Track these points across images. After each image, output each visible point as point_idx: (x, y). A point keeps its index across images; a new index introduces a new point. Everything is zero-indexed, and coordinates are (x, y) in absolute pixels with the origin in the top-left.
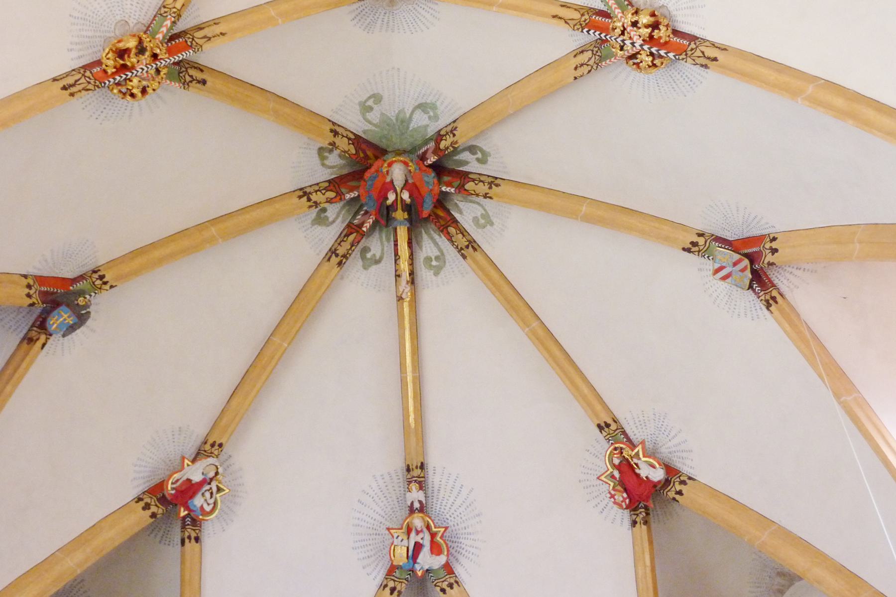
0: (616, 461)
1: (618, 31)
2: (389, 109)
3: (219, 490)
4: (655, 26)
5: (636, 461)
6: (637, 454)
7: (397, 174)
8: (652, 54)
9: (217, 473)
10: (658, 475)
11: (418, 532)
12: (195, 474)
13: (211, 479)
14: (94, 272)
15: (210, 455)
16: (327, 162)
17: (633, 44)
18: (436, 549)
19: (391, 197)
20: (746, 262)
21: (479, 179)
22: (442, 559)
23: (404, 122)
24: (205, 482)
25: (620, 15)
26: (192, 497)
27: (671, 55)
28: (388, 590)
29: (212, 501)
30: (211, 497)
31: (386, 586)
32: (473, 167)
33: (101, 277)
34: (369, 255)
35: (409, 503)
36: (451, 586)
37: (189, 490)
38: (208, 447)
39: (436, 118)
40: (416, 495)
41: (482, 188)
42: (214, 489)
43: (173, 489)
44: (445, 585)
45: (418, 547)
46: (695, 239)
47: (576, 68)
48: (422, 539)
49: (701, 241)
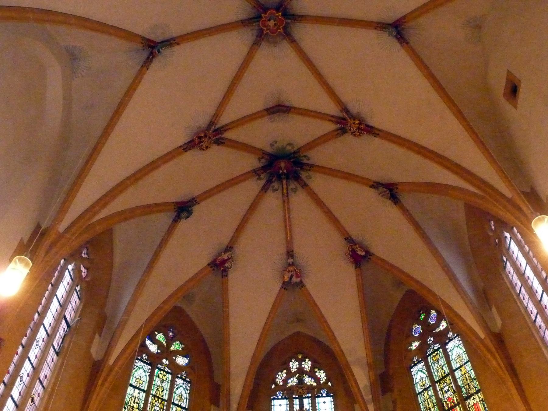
0: (351, 250)
1: (349, 125)
2: (279, 145)
4: (360, 124)
5: (356, 249)
6: (357, 247)
7: (283, 165)
8: (359, 132)
10: (363, 254)
11: (292, 272)
12: (225, 257)
13: (230, 258)
14: (193, 199)
15: (230, 251)
16: (261, 161)
17: (353, 129)
18: (297, 276)
19: (281, 172)
20: (388, 192)
21: (308, 165)
23: (284, 148)
24: (229, 259)
25: (349, 120)
26: (225, 264)
28: (283, 289)
29: (230, 265)
30: (230, 263)
32: (305, 161)
33: (195, 201)
34: (274, 188)
37: (224, 262)
38: (228, 248)
39: (293, 147)
40: (291, 260)
41: (308, 168)
42: (231, 261)
43: (219, 262)
44: (300, 287)
45: (292, 276)
46: (373, 184)
47: (336, 135)
48: (293, 273)
49: (375, 184)
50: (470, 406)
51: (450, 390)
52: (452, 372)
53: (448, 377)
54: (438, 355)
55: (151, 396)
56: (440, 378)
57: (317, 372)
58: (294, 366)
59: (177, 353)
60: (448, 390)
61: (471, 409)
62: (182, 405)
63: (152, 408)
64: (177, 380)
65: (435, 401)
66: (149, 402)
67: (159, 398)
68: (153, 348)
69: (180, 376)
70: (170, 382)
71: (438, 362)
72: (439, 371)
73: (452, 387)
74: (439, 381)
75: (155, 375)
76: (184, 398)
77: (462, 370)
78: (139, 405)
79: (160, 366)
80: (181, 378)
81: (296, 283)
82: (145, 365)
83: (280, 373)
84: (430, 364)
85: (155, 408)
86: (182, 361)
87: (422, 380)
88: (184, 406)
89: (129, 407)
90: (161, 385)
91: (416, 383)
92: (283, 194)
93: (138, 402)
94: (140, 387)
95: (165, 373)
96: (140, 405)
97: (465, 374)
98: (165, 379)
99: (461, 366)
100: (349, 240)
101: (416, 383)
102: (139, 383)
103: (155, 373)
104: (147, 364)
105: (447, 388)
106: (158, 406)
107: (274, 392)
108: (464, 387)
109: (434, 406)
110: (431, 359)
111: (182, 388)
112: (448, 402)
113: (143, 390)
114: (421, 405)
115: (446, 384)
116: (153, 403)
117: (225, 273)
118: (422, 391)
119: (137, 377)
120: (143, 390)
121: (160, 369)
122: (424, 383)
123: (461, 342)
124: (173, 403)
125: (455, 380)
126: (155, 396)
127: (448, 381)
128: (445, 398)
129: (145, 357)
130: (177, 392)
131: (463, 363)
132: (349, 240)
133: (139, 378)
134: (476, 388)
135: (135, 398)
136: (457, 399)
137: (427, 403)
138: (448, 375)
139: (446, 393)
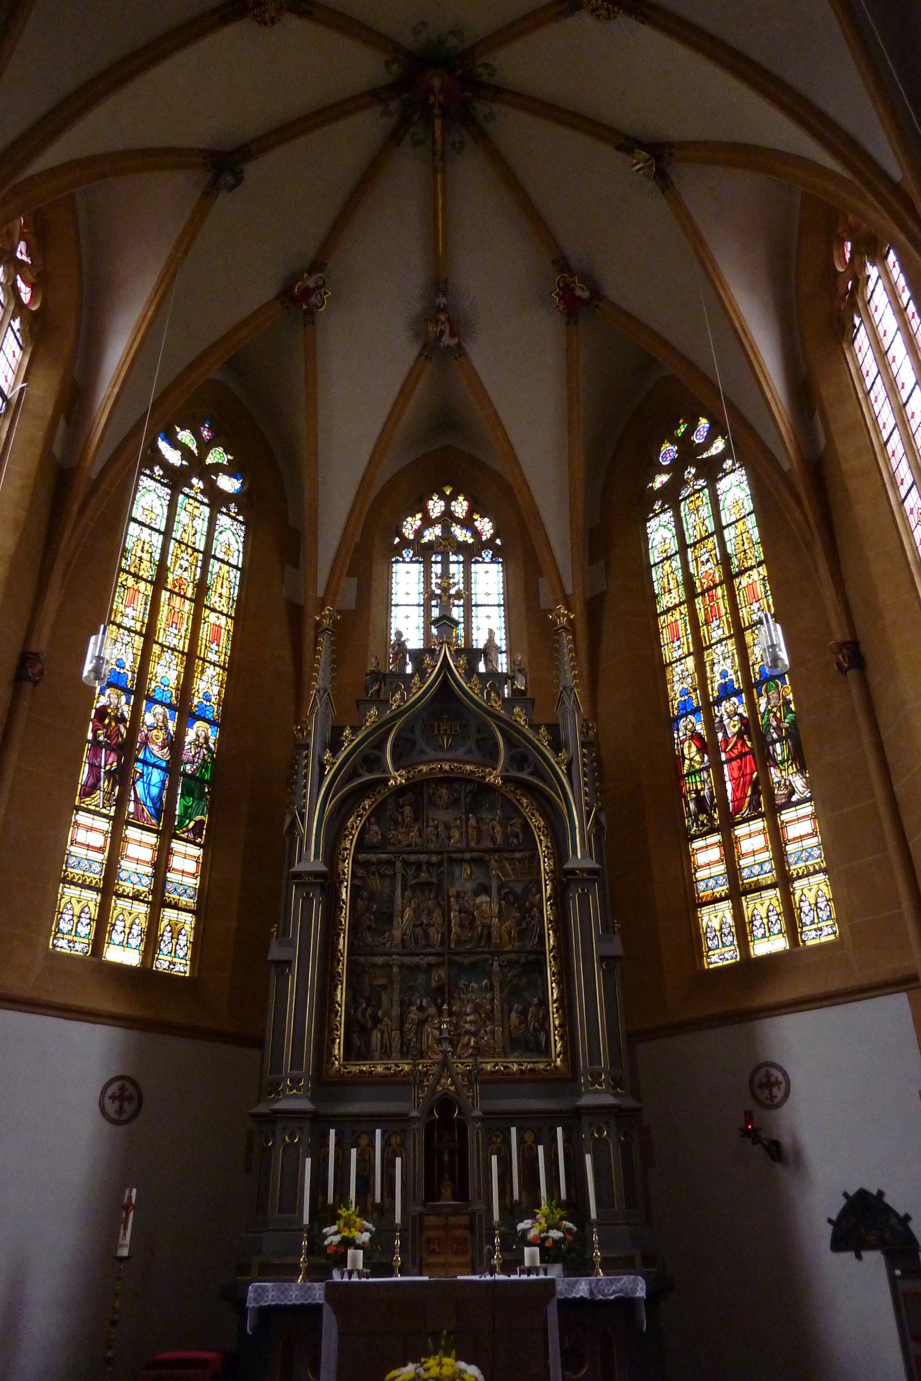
0: (562, 285)
3: (326, 293)
5: (573, 285)
7: (436, 83)
9: (324, 283)
10: (586, 295)
11: (443, 323)
12: (311, 283)
18: (453, 334)
19: (432, 98)
22: (456, 340)
24: (319, 287)
27: (621, 11)
28: (424, 357)
31: (423, 354)
35: (437, 304)
36: (460, 356)
37: (307, 293)
40: (442, 301)
45: (442, 332)
50: (741, 587)
51: (711, 560)
52: (720, 529)
53: (711, 538)
54: (700, 500)
55: (173, 541)
56: (696, 540)
57: (476, 520)
58: (436, 507)
59: (217, 468)
60: (708, 561)
61: (741, 593)
62: (230, 561)
63: (176, 562)
64: (219, 516)
65: (680, 579)
66: (171, 551)
67: (187, 546)
68: (174, 457)
69: (224, 510)
70: (206, 519)
71: (698, 513)
72: (697, 528)
73: (716, 555)
74: (694, 545)
75: (179, 505)
76: (233, 550)
77: (739, 527)
78: (151, 556)
79: (186, 490)
80: (228, 515)
81: (448, 346)
82: (159, 485)
83: (409, 519)
84: (683, 514)
85: (182, 562)
86: (228, 484)
87: (665, 541)
88: (235, 563)
89: (133, 557)
90: (190, 525)
91: (652, 547)
92: (434, 153)
93: (150, 551)
94: (152, 525)
95: (197, 504)
96: (153, 554)
97: (742, 534)
98: (198, 515)
99: (737, 521)
100: (562, 264)
101: (652, 547)
102: (149, 517)
103: (179, 502)
104: (163, 484)
105: (707, 556)
106: (187, 560)
107: (397, 551)
108: (736, 555)
109: (678, 587)
110: (686, 506)
111: (229, 533)
112: (703, 581)
113: (158, 531)
114: (655, 584)
115: (705, 550)
116: (177, 554)
117: (309, 317)
118: (662, 561)
119: (146, 507)
120: (158, 531)
122: (667, 547)
123: (745, 478)
124: (215, 557)
125: (722, 544)
126: (180, 543)
127: (710, 546)
128: (700, 573)
129: (158, 471)
130: (221, 538)
131: (742, 515)
132: (562, 264)
133: (150, 509)
134: (756, 557)
135: (144, 542)
136: (720, 576)
137: (666, 580)
138: (711, 535)
139: (703, 565)
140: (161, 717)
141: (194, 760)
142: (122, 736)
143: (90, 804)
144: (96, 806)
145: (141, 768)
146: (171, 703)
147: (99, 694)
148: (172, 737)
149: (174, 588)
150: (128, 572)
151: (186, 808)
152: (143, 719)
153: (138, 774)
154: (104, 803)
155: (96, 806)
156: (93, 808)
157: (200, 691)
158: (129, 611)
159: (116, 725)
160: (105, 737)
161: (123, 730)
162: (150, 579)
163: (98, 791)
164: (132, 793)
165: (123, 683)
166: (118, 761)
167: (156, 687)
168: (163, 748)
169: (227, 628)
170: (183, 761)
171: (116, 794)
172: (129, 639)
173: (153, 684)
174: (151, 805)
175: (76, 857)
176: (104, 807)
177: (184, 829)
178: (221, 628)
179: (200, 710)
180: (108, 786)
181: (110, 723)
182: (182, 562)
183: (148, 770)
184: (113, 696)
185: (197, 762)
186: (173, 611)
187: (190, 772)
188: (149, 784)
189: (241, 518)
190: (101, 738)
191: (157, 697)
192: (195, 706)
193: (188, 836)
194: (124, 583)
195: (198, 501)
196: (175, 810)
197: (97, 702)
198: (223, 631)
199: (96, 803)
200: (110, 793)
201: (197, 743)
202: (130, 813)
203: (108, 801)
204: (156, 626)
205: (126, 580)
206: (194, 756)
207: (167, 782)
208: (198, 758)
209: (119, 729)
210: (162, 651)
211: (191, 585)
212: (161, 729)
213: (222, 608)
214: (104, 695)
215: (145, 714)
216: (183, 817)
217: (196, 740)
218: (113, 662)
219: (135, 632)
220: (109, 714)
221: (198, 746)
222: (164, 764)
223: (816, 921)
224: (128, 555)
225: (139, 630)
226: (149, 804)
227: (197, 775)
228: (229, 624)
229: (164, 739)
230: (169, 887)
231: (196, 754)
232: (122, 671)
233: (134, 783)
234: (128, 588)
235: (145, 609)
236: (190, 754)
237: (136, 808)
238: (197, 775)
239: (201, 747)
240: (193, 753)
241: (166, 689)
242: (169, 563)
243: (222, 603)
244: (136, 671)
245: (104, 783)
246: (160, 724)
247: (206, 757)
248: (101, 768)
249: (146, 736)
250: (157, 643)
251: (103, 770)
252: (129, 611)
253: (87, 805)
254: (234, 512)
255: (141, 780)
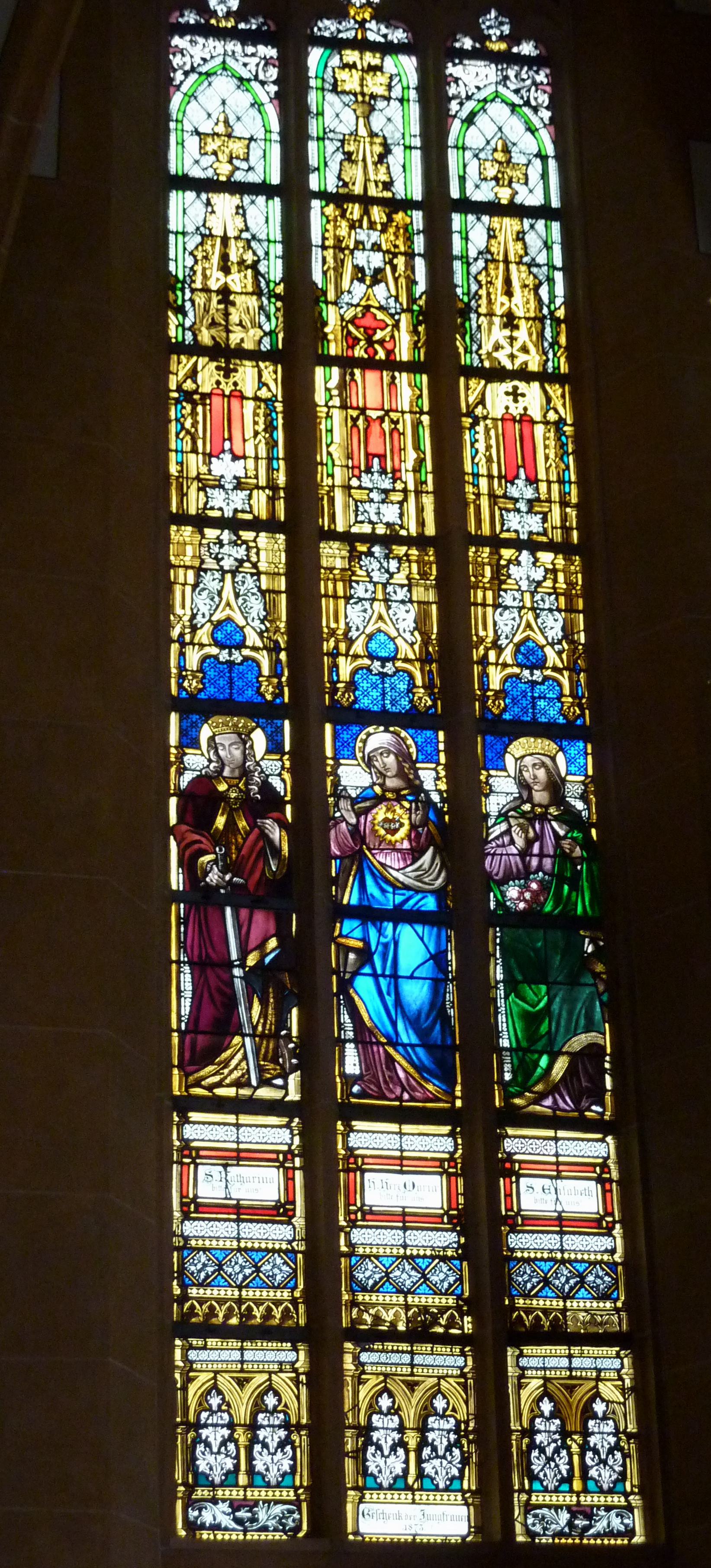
55: (316, 204)
62: (518, 200)
63: (340, 265)
64: (451, 70)
66: (316, 237)
67: (366, 201)
69: (467, 43)
70: (413, 95)
75: (312, 83)
76: (523, 160)
78: (257, 273)
79: (328, 27)
80: (481, 54)
82: (234, 46)
85: (361, 258)
88: (535, 200)
89: (200, 299)
90: (362, 131)
93: (249, 258)
94: (239, 176)
95: (371, 58)
96: (262, 268)
98: (381, 91)
102: (223, 157)
103: (312, 73)
104: (246, 38)
106: (376, 247)
111: (498, 110)
113: (263, 189)
116: (338, 240)
119: (206, 127)
120: (263, 189)
121: (335, 44)
124: (466, 206)
130: (474, 138)
133: (221, 129)
135: (225, 240)
140: (391, 760)
141: (527, 866)
142: (276, 851)
143: (219, 1085)
144: (237, 1084)
145: (358, 933)
146: (414, 707)
147: (181, 746)
148: (440, 813)
149: (352, 347)
150: (196, 349)
151: (531, 1020)
152: (336, 783)
153: (352, 956)
154: (261, 1070)
155: (237, 1084)
156: (231, 1092)
157: (503, 642)
158: (224, 467)
159: (253, 825)
160: (224, 871)
161: (276, 833)
162: (266, 345)
163: (237, 1039)
164: (346, 1018)
165: (250, 693)
166: (282, 934)
167: (354, 673)
168: (415, 853)
169: (552, 416)
170: (489, 876)
171: (295, 1033)
172: (241, 552)
173: (345, 668)
174: (414, 1040)
175: (205, 1250)
176: (264, 1082)
177: (539, 1087)
178: (533, 422)
179: (515, 701)
180: (264, 1014)
181: (231, 824)
182: (361, 258)
183: (380, 932)
184: (225, 740)
185: (540, 868)
186: (361, 423)
187: (522, 905)
188: (395, 976)
189: (527, 49)
190: (213, 877)
191: (365, 703)
192: (497, 693)
193: (555, 1107)
194: (189, 385)
195: (374, 47)
196: (497, 1035)
197: (180, 772)
198: (539, 430)
199: (236, 1074)
200: (276, 1036)
201: (527, 807)
202: (348, 1080)
203: (275, 1060)
204: (317, 486)
205: (193, 374)
206: (525, 853)
207: (451, 956)
208: (541, 855)
209: (264, 836)
210: (354, 556)
211: (404, 319)
212: (399, 799)
213: (521, 358)
214: (196, 744)
215: (337, 765)
216: (526, 1051)
217: (521, 800)
218: (203, 635)
219: (256, 525)
220: (223, 796)
221: (530, 818)
222: (430, 904)
223: (243, 1479)
224: (181, 297)
225: (264, 515)
226: (406, 1036)
227: (548, 908)
228: (558, 403)
229: (413, 827)
230: (523, 1277)
231: (529, 843)
232: (237, 656)
233: (346, 985)
234: (204, 396)
235: (272, 444)
236: (513, 850)
237: (366, 1060)
238: (548, 908)
239: (543, 818)
240: (520, 842)
241: (389, 668)
242: (317, 277)
243: (517, 345)
244: (282, 641)
245: (249, 1008)
246: (391, 783)
247: (566, 844)
248: (230, 965)
249: (355, 831)
250: (332, 535)
251: (237, 972)
252: (224, 467)
253: (210, 1088)
254: (501, 38)
255: (367, 970)
